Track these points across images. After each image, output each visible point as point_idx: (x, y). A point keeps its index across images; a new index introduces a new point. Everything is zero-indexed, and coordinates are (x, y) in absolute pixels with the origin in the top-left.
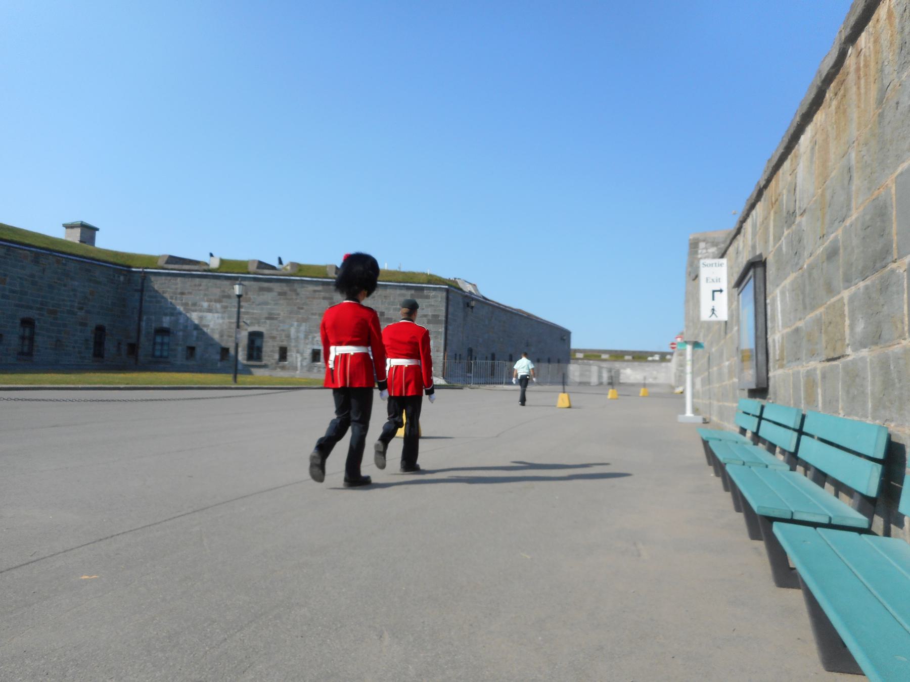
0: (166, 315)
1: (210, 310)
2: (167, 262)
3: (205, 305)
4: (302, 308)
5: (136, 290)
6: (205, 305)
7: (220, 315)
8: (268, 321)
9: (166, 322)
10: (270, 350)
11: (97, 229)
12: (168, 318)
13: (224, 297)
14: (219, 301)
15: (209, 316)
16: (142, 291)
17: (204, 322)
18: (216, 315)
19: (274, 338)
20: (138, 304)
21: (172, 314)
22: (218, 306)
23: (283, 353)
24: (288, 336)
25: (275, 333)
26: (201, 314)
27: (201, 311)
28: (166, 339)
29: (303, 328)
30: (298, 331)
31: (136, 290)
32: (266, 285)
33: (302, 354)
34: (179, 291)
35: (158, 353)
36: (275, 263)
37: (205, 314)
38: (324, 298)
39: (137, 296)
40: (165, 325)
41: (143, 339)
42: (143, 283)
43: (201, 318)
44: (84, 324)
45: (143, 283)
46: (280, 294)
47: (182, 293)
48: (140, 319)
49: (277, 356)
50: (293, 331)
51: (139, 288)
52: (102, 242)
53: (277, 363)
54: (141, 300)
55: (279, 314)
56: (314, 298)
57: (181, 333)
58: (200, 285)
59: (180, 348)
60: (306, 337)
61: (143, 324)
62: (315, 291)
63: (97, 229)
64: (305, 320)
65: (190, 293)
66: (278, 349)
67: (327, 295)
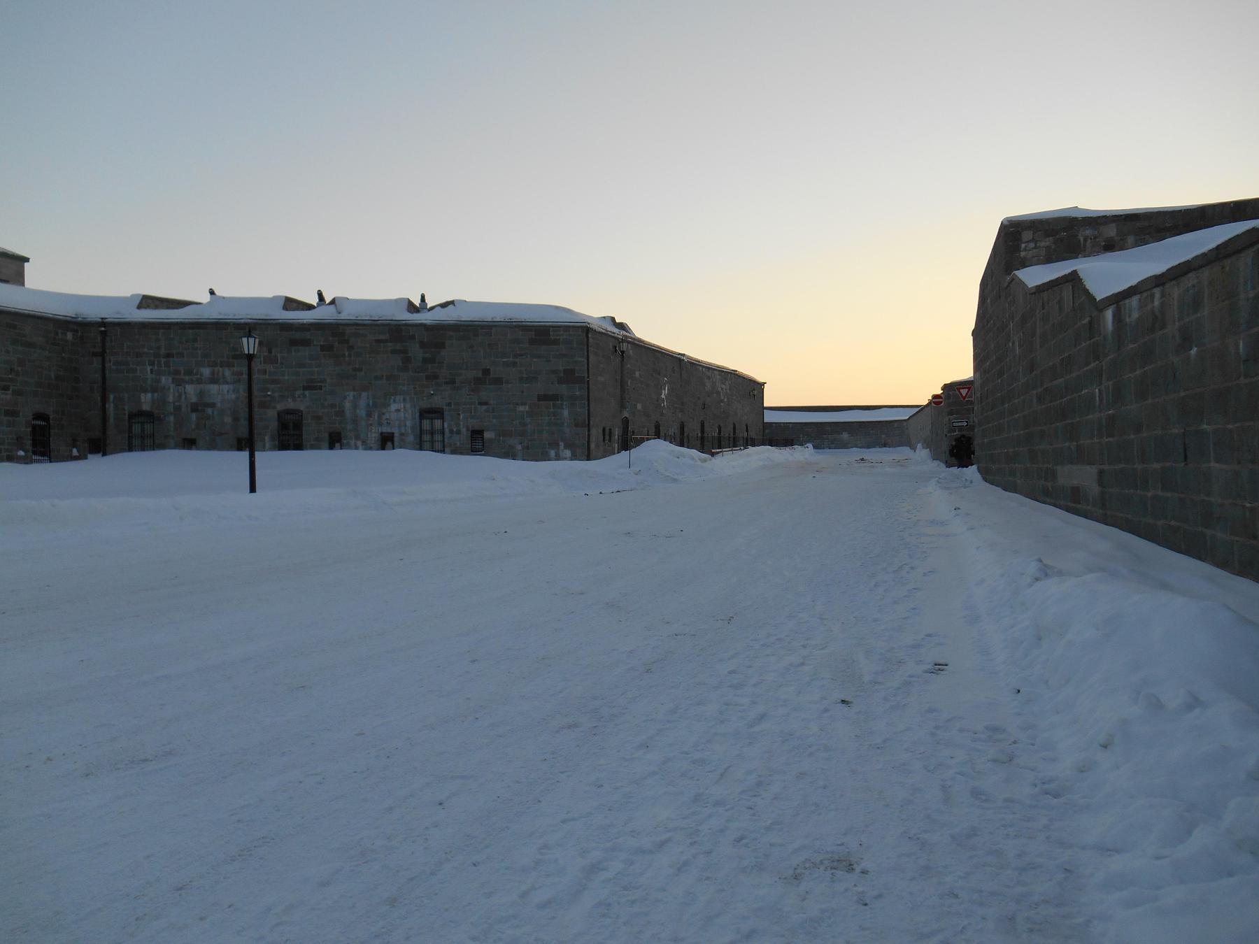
0: (146, 391)
1: (213, 380)
2: (139, 307)
3: (206, 371)
4: (360, 370)
5: (95, 354)
6: (206, 371)
7: (231, 387)
8: (307, 393)
9: (146, 402)
11: (27, 260)
12: (149, 395)
14: (229, 365)
15: (214, 388)
16: (102, 354)
21: (154, 390)
22: (227, 373)
24: (341, 413)
26: (199, 387)
27: (200, 381)
28: (149, 428)
29: (362, 403)
30: (355, 407)
31: (95, 354)
34: (163, 351)
36: (314, 300)
38: (393, 352)
39: (97, 363)
40: (146, 407)
42: (103, 341)
44: (12, 413)
45: (103, 341)
46: (323, 348)
47: (169, 355)
48: (104, 399)
50: (347, 405)
51: (99, 350)
52: (35, 278)
54: (104, 368)
55: (323, 381)
58: (195, 340)
60: (369, 415)
61: (110, 407)
62: (378, 341)
63: (27, 260)
65: (181, 355)
67: (398, 346)
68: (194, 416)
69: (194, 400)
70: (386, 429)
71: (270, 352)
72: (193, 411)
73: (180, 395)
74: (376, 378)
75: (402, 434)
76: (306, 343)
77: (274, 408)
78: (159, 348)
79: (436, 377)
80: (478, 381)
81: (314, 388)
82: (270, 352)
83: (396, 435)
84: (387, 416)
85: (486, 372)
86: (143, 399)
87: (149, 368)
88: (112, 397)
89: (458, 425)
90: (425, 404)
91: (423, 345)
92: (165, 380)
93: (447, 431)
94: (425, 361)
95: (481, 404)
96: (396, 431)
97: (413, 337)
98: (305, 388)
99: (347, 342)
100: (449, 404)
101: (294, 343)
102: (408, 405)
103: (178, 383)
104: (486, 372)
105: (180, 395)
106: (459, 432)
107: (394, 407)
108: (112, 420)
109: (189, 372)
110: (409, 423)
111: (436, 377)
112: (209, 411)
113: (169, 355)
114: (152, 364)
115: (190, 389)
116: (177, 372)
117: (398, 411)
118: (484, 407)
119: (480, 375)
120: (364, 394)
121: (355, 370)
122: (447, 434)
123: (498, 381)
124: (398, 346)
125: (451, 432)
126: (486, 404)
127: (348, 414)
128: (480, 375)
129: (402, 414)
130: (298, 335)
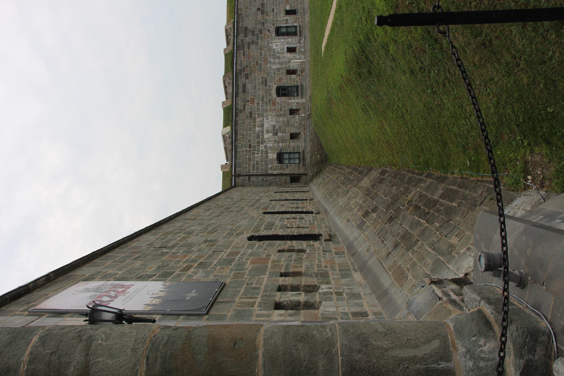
0: (267, 157)
4: (257, 62)
5: (249, 180)
7: (265, 118)
9: (273, 156)
10: (288, 80)
12: (269, 155)
13: (251, 117)
14: (255, 118)
15: (266, 126)
16: (249, 176)
17: (271, 129)
18: (265, 121)
19: (280, 79)
20: (260, 178)
21: (267, 152)
22: (258, 120)
23: (291, 72)
24: (278, 70)
26: (265, 132)
27: (263, 132)
30: (275, 63)
31: (249, 180)
32: (241, 89)
33: (292, 59)
34: (248, 149)
35: (297, 161)
37: (265, 128)
38: (249, 48)
39: (252, 179)
40: (275, 156)
41: (287, 171)
42: (243, 176)
43: (268, 132)
45: (243, 176)
46: (247, 78)
47: (250, 146)
50: (274, 67)
51: (247, 177)
53: (299, 76)
55: (262, 77)
56: (249, 55)
57: (280, 144)
58: (243, 135)
59: (292, 144)
62: (244, 55)
64: (266, 60)
65: (250, 140)
67: (246, 46)
68: (279, 134)
69: (271, 134)
70: (285, 50)
71: (248, 101)
72: (277, 135)
73: (270, 141)
74: (261, 55)
75: (288, 43)
76: (244, 86)
77: (275, 98)
78: (246, 151)
79: (261, 30)
80: (263, 13)
81: (266, 81)
82: (248, 101)
83: (288, 46)
84: (279, 50)
85: (258, 9)
86: (271, 157)
87: (256, 155)
88: (270, 172)
89: (283, 20)
91: (246, 36)
92: (262, 147)
93: (286, 25)
94: (253, 35)
95: (273, 11)
96: (286, 46)
97: (242, 40)
98: (266, 85)
99: (244, 68)
100: (274, 24)
101: (244, 91)
102: (274, 41)
103: (263, 142)
104: (258, 9)
105: (270, 141)
106: (287, 20)
107: (275, 47)
108: (281, 172)
109: (258, 137)
110: (283, 41)
111: (261, 30)
112: (277, 127)
113: (250, 146)
114: (254, 154)
115: (266, 136)
116: (258, 142)
117: (277, 45)
118: (275, 10)
119: (260, 12)
120: (269, 60)
121: (257, 64)
122: (288, 25)
123: (263, 5)
124: (246, 46)
125: (286, 23)
127: (278, 66)
128: (260, 12)
129: (278, 44)
130: (241, 89)
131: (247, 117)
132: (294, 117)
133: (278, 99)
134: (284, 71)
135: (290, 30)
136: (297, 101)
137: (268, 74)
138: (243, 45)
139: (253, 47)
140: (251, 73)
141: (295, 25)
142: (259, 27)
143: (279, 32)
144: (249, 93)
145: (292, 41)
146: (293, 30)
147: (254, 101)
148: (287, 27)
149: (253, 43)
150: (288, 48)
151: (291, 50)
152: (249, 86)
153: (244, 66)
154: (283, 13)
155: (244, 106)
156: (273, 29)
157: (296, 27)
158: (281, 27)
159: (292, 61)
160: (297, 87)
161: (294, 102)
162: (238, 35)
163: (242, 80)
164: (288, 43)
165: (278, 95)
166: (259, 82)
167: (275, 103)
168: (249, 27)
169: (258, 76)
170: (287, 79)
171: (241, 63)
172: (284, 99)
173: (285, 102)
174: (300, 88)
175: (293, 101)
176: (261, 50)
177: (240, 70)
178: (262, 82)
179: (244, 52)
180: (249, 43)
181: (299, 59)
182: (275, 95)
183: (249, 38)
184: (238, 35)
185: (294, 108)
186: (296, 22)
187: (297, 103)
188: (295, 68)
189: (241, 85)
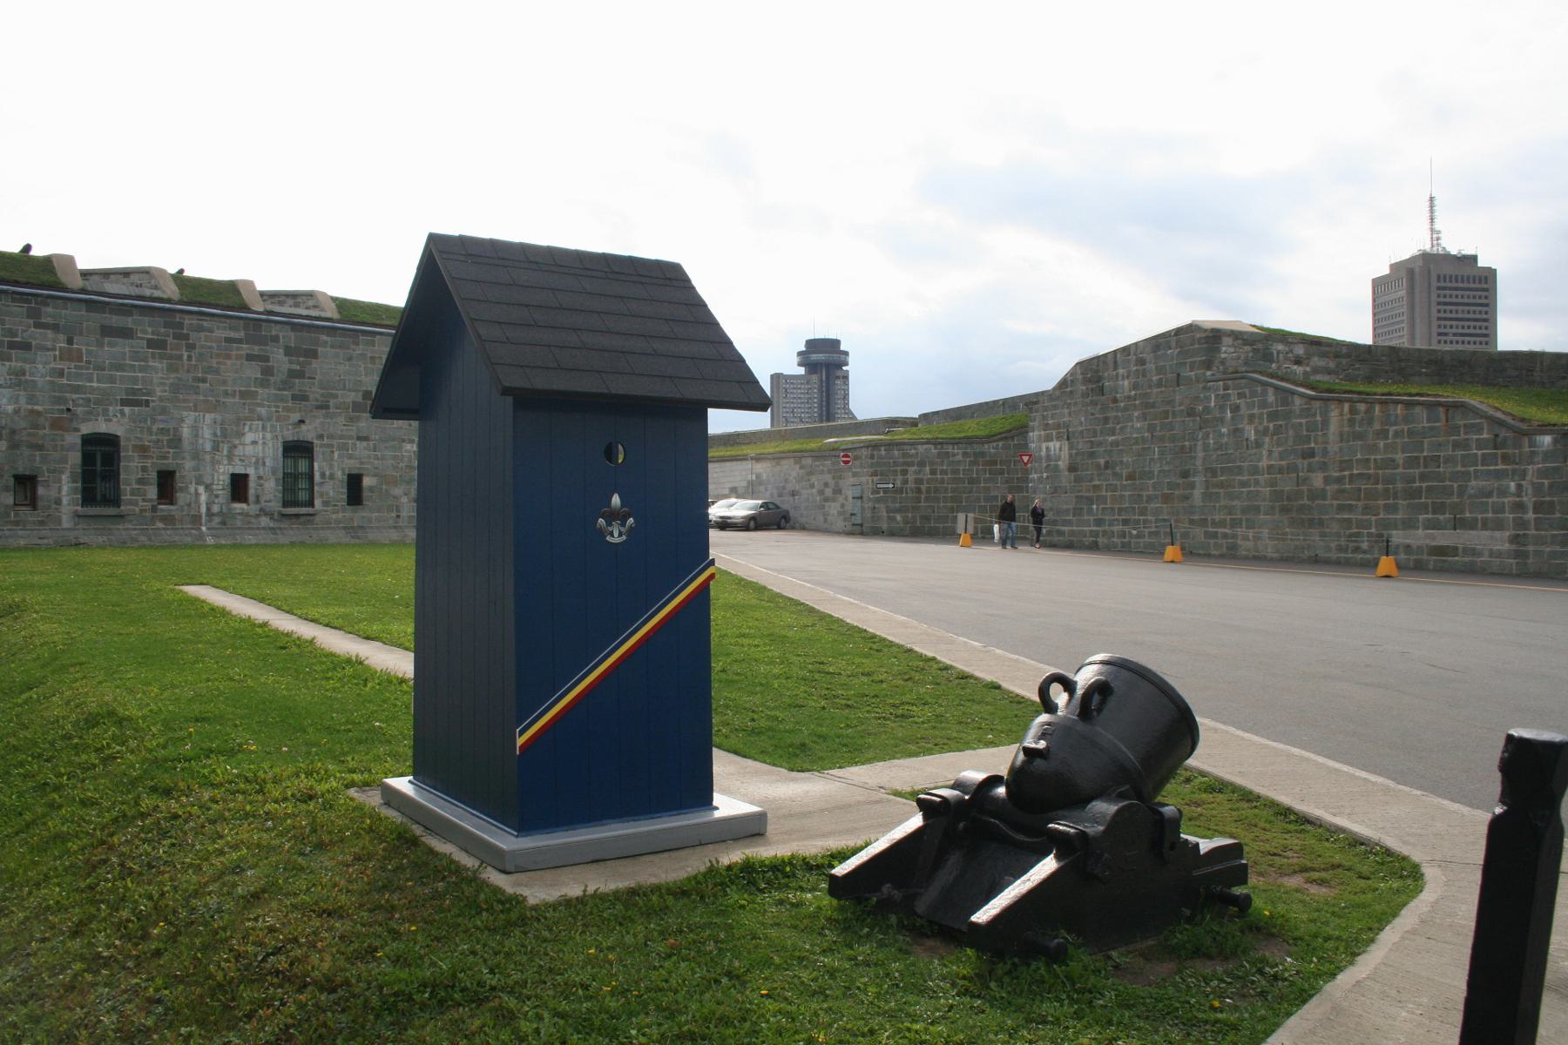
4: (204, 380)
8: (127, 410)
19: (143, 450)
23: (167, 484)
24: (176, 442)
25: (147, 440)
32: (115, 320)
38: (250, 358)
49: (152, 492)
53: (154, 509)
56: (228, 357)
62: (229, 340)
66: (154, 475)
67: (256, 350)
70: (239, 470)
71: (70, 341)
75: (260, 478)
76: (127, 333)
77: (77, 430)
81: (138, 403)
82: (70, 341)
90: (290, 435)
91: (288, 351)
95: (359, 438)
96: (251, 471)
97: (275, 339)
98: (124, 403)
99: (187, 337)
100: (321, 437)
101: (107, 331)
106: (332, 477)
107: (249, 437)
117: (254, 443)
124: (256, 350)
125: (323, 475)
126: (366, 439)
130: (115, 320)
131: (13, 334)
132: (7, 489)
133: (74, 439)
134: (170, 463)
135: (303, 484)
136: (65, 501)
137: (164, 411)
138: (262, 341)
139: (253, 371)
140: (171, 357)
141: (317, 502)
142: (315, 393)
143: (297, 450)
144: (100, 345)
145: (267, 488)
146: (303, 496)
147: (71, 360)
148: (311, 477)
149: (268, 371)
150: (246, 476)
151: (239, 487)
152: (122, 347)
153: (193, 335)
154: (352, 465)
155: (55, 328)
156: (307, 433)
157: (311, 504)
158: (311, 460)
159: (201, 489)
160: (115, 501)
161: (63, 490)
162: (294, 327)
163: (147, 329)
164: (260, 478)
165: (90, 441)
166: (135, 380)
167: (61, 428)
168: (315, 364)
169: (157, 376)
170: (144, 469)
171: (201, 329)
172: (75, 458)
173: (64, 460)
174: (111, 511)
175: (65, 489)
176: (243, 395)
177: (181, 326)
178: (134, 392)
179: (240, 341)
180: (267, 359)
181: (208, 509)
182: (86, 429)
183: (279, 358)
184: (294, 327)
185: (41, 491)
186: (326, 503)
187: (58, 502)
188: (182, 498)
189: (129, 322)
